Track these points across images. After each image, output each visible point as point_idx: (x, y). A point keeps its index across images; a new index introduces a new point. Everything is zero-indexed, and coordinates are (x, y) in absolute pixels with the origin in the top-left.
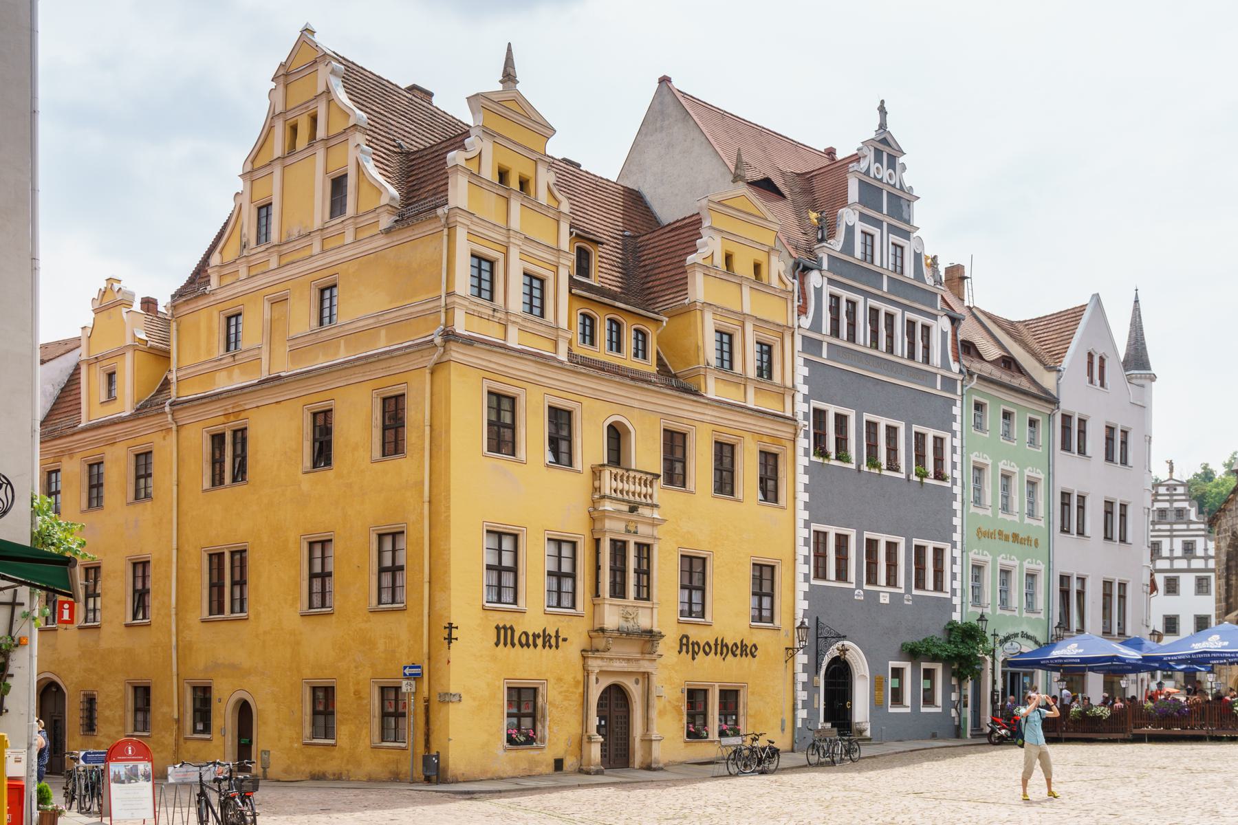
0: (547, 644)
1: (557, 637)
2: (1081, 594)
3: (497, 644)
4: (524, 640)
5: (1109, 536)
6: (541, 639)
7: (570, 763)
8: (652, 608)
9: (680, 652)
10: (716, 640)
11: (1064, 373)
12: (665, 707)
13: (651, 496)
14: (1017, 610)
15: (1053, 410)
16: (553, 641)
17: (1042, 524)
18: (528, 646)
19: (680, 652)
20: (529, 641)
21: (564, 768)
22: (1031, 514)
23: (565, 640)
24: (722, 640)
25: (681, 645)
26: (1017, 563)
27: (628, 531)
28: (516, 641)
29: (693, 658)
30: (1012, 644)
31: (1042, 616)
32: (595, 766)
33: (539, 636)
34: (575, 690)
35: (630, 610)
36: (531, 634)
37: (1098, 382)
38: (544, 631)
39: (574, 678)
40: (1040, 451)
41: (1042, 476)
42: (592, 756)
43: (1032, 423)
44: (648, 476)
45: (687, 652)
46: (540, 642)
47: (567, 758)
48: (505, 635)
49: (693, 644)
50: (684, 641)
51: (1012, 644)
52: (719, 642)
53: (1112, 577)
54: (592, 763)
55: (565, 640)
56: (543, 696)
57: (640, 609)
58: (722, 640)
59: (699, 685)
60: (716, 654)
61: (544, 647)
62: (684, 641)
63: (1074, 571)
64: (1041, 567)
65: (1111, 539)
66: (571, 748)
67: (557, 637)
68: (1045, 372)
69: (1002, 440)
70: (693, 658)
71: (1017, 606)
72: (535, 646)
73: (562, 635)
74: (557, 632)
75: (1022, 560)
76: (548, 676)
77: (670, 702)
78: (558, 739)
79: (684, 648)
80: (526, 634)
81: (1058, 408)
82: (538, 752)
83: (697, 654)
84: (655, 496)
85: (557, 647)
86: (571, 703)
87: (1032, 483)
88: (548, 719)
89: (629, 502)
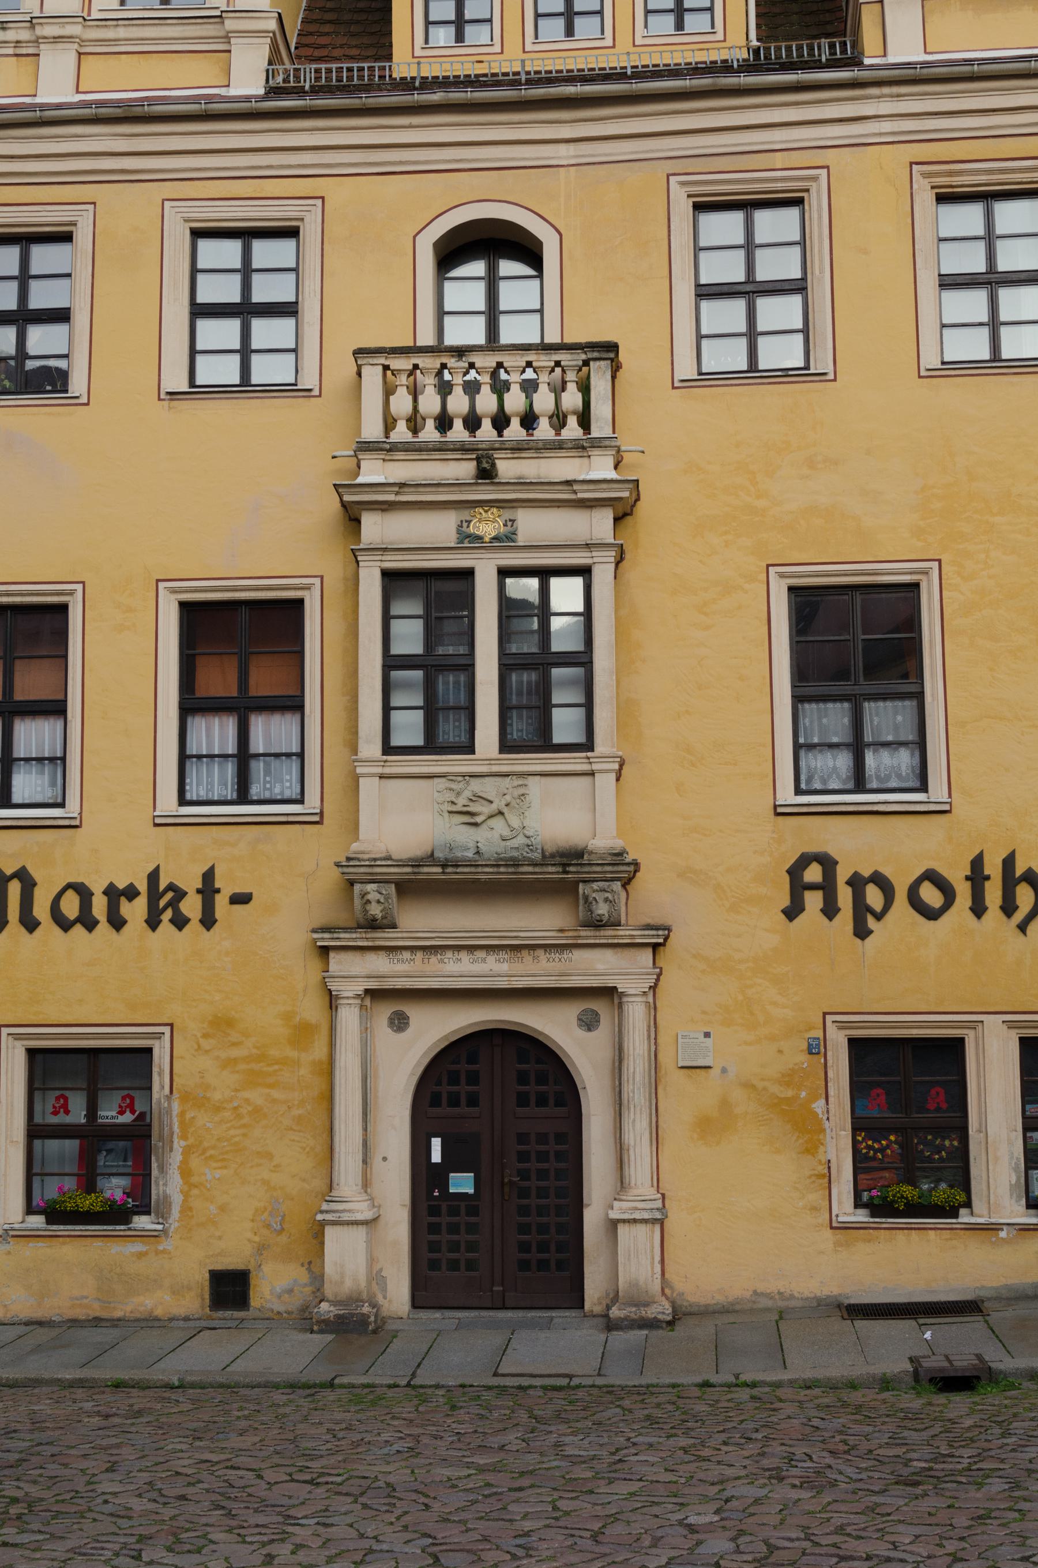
0: (168, 914)
1: (208, 889)
4: (71, 906)
6: (141, 904)
7: (281, 1283)
8: (592, 774)
9: (793, 911)
10: (977, 863)
12: (725, 1104)
13: (585, 420)
16: (191, 906)
18: (90, 924)
19: (793, 911)
21: (255, 1302)
23: (241, 899)
24: (1009, 863)
25: (798, 888)
27: (468, 540)
28: (41, 910)
29: (862, 932)
32: (334, 1303)
33: (131, 893)
34: (293, 1054)
35: (488, 788)
36: (97, 888)
38: (153, 877)
39: (287, 1017)
42: (329, 1269)
44: (564, 357)
45: (830, 910)
46: (135, 911)
47: (267, 1269)
49: (857, 883)
50: (813, 873)
52: (993, 868)
54: (329, 1291)
55: (241, 899)
56: (161, 1074)
57: (532, 781)
58: (1009, 863)
59: (920, 1025)
60: (978, 909)
61: (153, 923)
62: (813, 873)
66: (283, 1239)
67: (208, 889)
70: (862, 932)
72: (117, 923)
73: (226, 885)
74: (209, 876)
76: (173, 1011)
77: (748, 1085)
78: (223, 1209)
79: (814, 900)
80: (83, 892)
82: (138, 1247)
83: (879, 917)
84: (601, 410)
85: (208, 921)
86: (276, 1094)
88: (178, 1145)
89: (463, 448)
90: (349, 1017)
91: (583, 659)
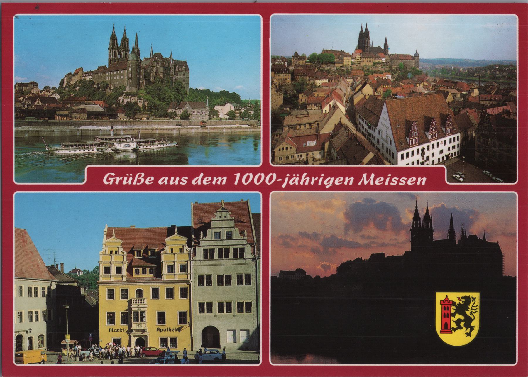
1: (123, 329)
3: (109, 331)
4: (115, 330)
9: (157, 331)
20: (116, 331)
23: (125, 330)
28: (114, 331)
45: (159, 331)
46: (119, 331)
48: (111, 330)
60: (167, 331)
67: (123, 329)
72: (118, 331)
73: (124, 329)
80: (116, 330)
90: (132, 337)
91: (145, 317)
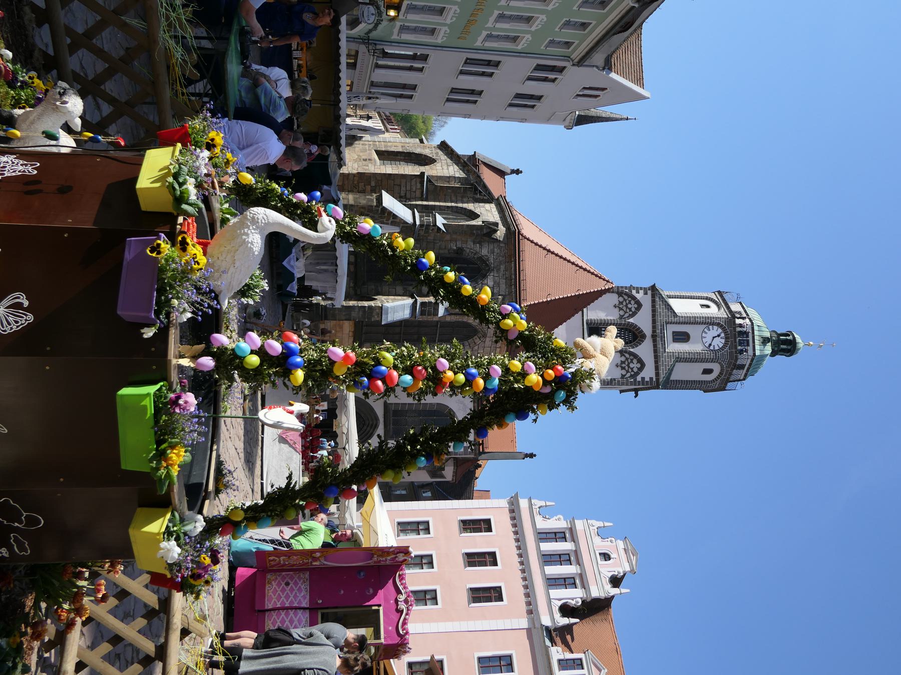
2: (411, 69)
5: (453, 90)
11: (602, 72)
14: (404, 18)
15: (573, 61)
17: (478, 44)
22: (489, 36)
26: (448, 21)
30: (373, 14)
31: (395, 37)
37: (581, 93)
40: (542, 48)
41: (520, 47)
43: (568, 44)
51: (373, 14)
53: (419, 91)
63: (428, 66)
64: (439, 39)
65: (451, 92)
68: (605, 56)
69: (565, 19)
71: (408, 18)
75: (450, 26)
81: (574, 65)
87: (515, 39)
